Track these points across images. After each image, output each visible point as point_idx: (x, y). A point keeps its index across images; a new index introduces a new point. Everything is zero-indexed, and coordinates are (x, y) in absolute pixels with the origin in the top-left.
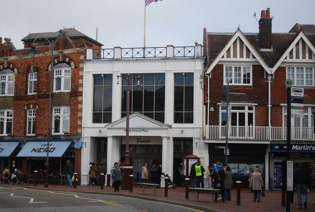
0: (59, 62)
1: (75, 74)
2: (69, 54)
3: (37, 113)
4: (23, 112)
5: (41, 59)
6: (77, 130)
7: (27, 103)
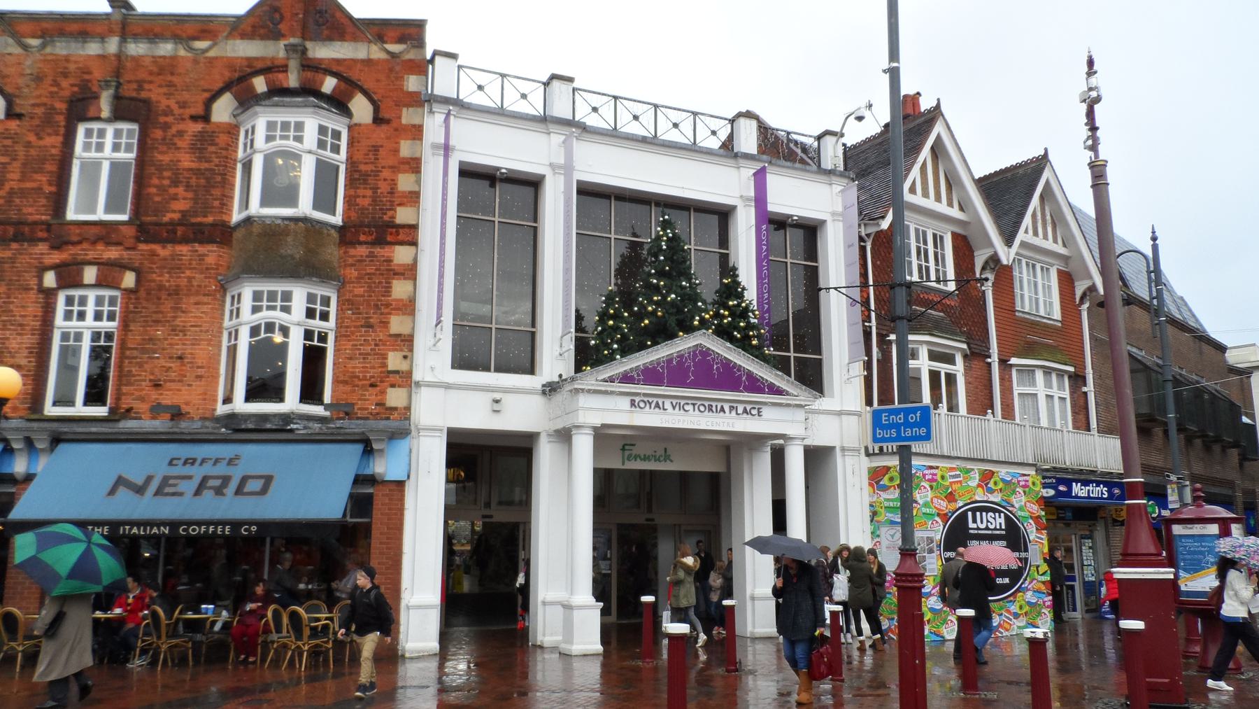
0: (278, 92)
1: (376, 149)
2: (338, 61)
3: (136, 308)
4: (32, 295)
5: (166, 67)
6: (383, 392)
7: (56, 257)
